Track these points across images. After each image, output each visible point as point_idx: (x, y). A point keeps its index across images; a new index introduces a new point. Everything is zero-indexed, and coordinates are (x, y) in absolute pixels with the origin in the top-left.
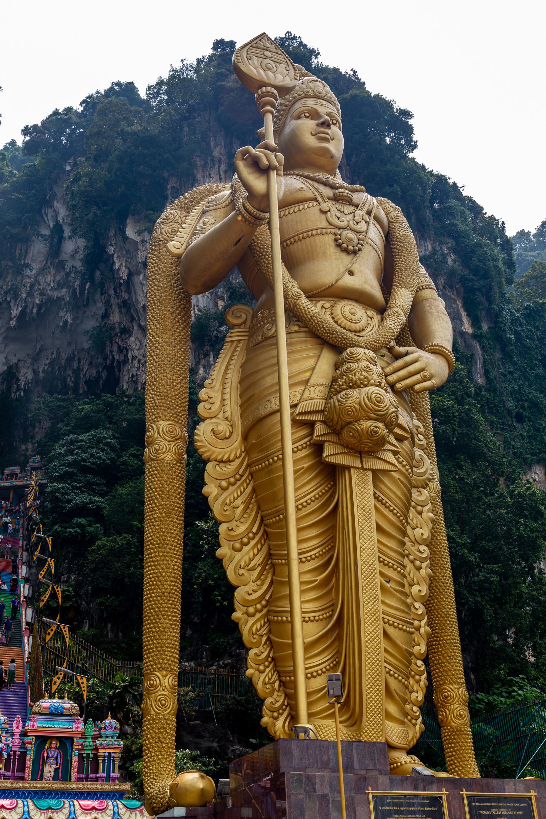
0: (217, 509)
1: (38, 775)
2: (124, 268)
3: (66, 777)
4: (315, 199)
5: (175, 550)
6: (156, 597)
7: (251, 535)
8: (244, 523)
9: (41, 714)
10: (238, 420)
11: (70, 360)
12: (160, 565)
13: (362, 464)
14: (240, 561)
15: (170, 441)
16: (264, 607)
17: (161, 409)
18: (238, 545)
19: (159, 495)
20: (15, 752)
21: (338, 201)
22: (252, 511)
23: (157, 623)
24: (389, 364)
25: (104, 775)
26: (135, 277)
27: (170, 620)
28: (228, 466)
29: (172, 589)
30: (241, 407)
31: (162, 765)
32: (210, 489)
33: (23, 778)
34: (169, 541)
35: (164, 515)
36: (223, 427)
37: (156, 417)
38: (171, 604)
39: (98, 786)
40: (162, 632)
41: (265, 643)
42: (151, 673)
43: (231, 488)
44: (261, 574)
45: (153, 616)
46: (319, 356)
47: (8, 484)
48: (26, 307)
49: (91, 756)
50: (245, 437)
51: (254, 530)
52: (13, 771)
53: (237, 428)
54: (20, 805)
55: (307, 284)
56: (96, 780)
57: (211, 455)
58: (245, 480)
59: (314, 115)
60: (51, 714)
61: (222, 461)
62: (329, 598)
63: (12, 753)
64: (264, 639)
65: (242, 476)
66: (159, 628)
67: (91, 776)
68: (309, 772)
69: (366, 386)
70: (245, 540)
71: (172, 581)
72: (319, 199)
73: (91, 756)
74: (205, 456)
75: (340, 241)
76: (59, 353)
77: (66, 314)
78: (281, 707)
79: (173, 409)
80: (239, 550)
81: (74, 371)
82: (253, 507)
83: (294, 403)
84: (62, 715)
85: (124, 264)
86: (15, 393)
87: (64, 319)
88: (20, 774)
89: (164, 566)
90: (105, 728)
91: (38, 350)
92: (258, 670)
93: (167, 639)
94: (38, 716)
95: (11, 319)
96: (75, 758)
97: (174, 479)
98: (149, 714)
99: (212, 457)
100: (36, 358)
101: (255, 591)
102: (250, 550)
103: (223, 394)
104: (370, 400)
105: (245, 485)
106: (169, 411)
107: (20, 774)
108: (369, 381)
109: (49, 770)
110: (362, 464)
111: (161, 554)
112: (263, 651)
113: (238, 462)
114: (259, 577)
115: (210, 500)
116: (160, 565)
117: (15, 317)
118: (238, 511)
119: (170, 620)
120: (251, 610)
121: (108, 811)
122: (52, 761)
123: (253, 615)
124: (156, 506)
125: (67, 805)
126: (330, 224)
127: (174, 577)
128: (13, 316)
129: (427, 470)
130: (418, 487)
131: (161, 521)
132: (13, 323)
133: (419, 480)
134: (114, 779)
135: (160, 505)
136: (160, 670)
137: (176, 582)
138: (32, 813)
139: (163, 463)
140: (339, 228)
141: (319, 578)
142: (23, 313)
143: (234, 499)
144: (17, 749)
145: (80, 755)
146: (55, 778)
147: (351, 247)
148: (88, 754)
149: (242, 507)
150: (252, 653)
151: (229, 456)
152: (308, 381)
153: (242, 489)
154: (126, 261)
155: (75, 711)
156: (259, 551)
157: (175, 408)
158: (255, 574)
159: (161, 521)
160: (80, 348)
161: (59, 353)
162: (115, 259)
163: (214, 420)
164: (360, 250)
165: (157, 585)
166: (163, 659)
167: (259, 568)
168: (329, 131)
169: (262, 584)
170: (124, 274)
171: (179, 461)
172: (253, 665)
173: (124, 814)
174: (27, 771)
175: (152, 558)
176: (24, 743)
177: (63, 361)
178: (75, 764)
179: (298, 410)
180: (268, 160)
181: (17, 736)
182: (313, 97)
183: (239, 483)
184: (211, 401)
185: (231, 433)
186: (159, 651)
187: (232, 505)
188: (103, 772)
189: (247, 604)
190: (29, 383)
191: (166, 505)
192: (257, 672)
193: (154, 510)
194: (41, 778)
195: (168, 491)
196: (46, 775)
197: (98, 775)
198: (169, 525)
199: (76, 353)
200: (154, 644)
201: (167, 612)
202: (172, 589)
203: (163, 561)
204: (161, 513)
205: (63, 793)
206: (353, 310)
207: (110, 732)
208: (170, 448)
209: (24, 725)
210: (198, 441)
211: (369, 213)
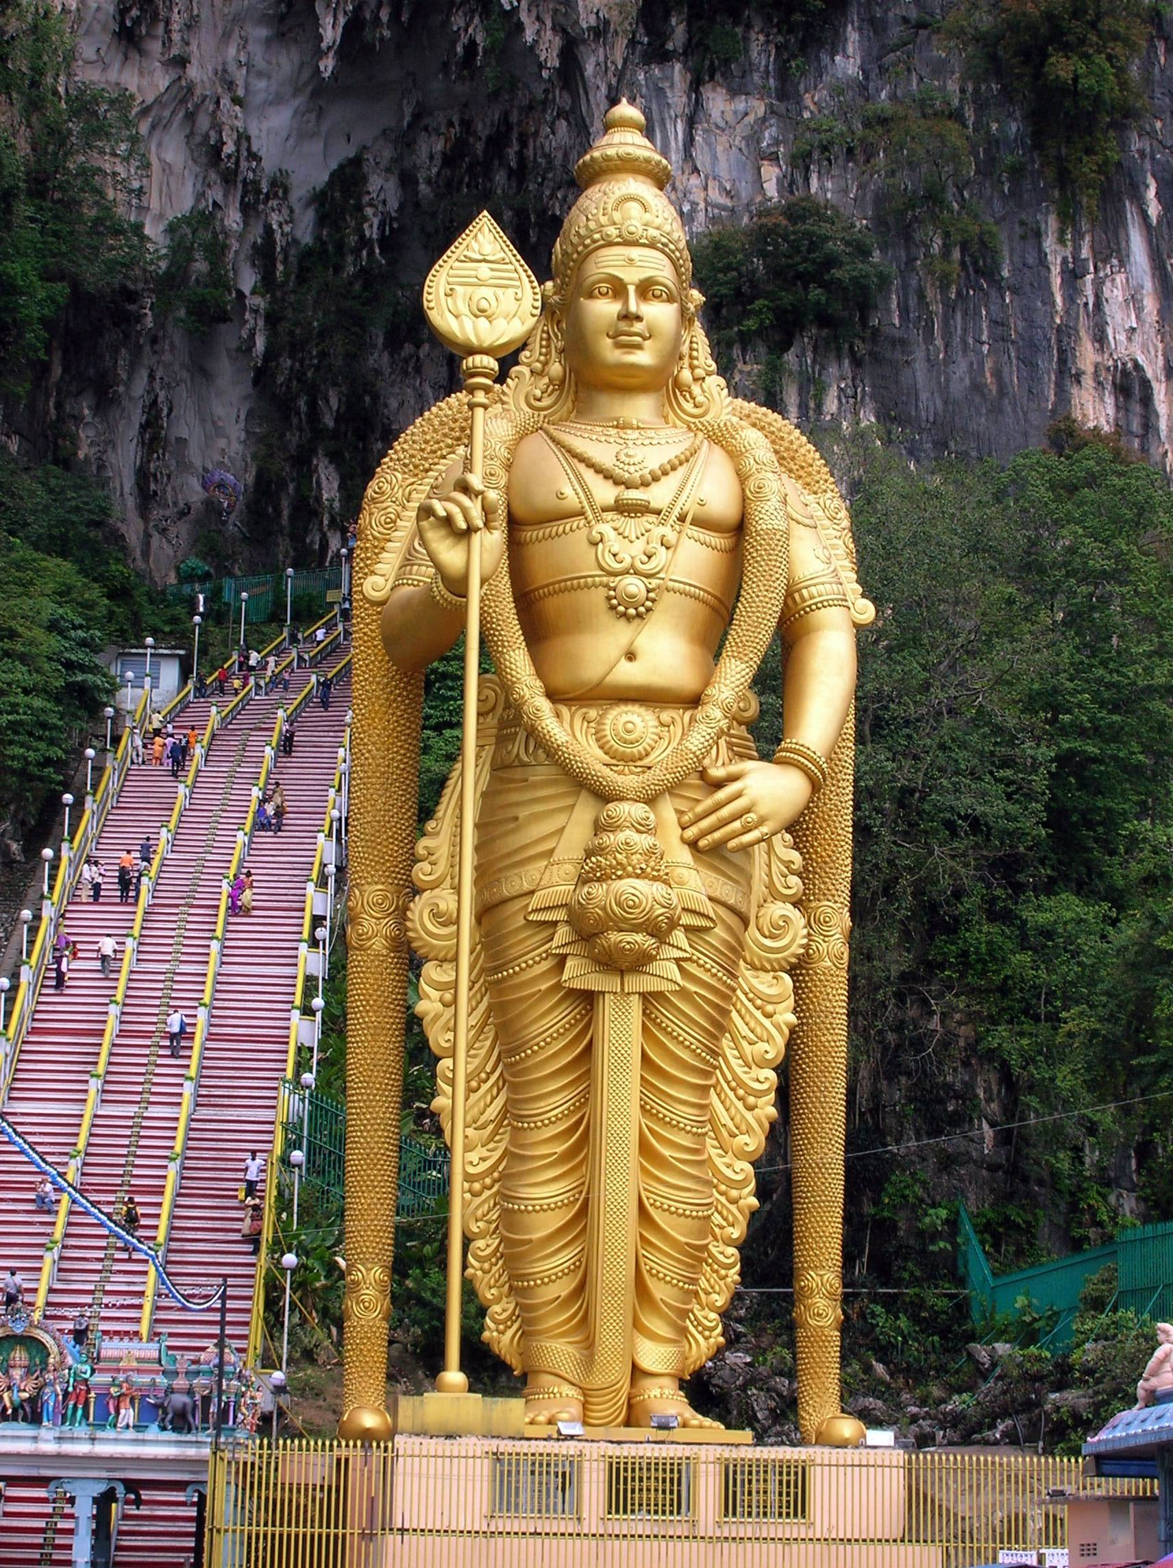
2: (549, 34)
4: (582, 513)
7: (483, 1075)
11: (497, 143)
13: (622, 984)
16: (495, 1181)
21: (621, 513)
24: (698, 801)
26: (582, 48)
44: (495, 1133)
46: (573, 806)
48: (358, 9)
55: (560, 680)
59: (618, 289)
62: (578, 1174)
69: (620, 877)
72: (589, 513)
75: (614, 602)
76: (467, 124)
77: (472, 19)
78: (509, 1318)
81: (511, 173)
82: (490, 1032)
85: (549, 24)
86: (357, 252)
87: (464, 40)
91: (407, 119)
95: (320, 54)
100: (405, 140)
101: (483, 1159)
104: (619, 904)
108: (624, 869)
110: (622, 984)
114: (491, 1139)
117: (329, 48)
120: (477, 1186)
126: (602, 569)
128: (324, 45)
129: (793, 941)
130: (774, 970)
132: (327, 65)
133: (777, 960)
140: (615, 574)
141: (560, 1149)
142: (354, 28)
147: (632, 611)
152: (551, 852)
154: (556, 11)
160: (525, 102)
161: (467, 124)
162: (524, 17)
163: (437, 891)
164: (649, 610)
167: (491, 1127)
168: (638, 327)
170: (550, 53)
177: (479, 147)
179: (535, 902)
180: (466, 520)
182: (618, 244)
184: (432, 858)
190: (392, 219)
192: (479, 1273)
199: (514, 118)
206: (630, 726)
211: (682, 519)
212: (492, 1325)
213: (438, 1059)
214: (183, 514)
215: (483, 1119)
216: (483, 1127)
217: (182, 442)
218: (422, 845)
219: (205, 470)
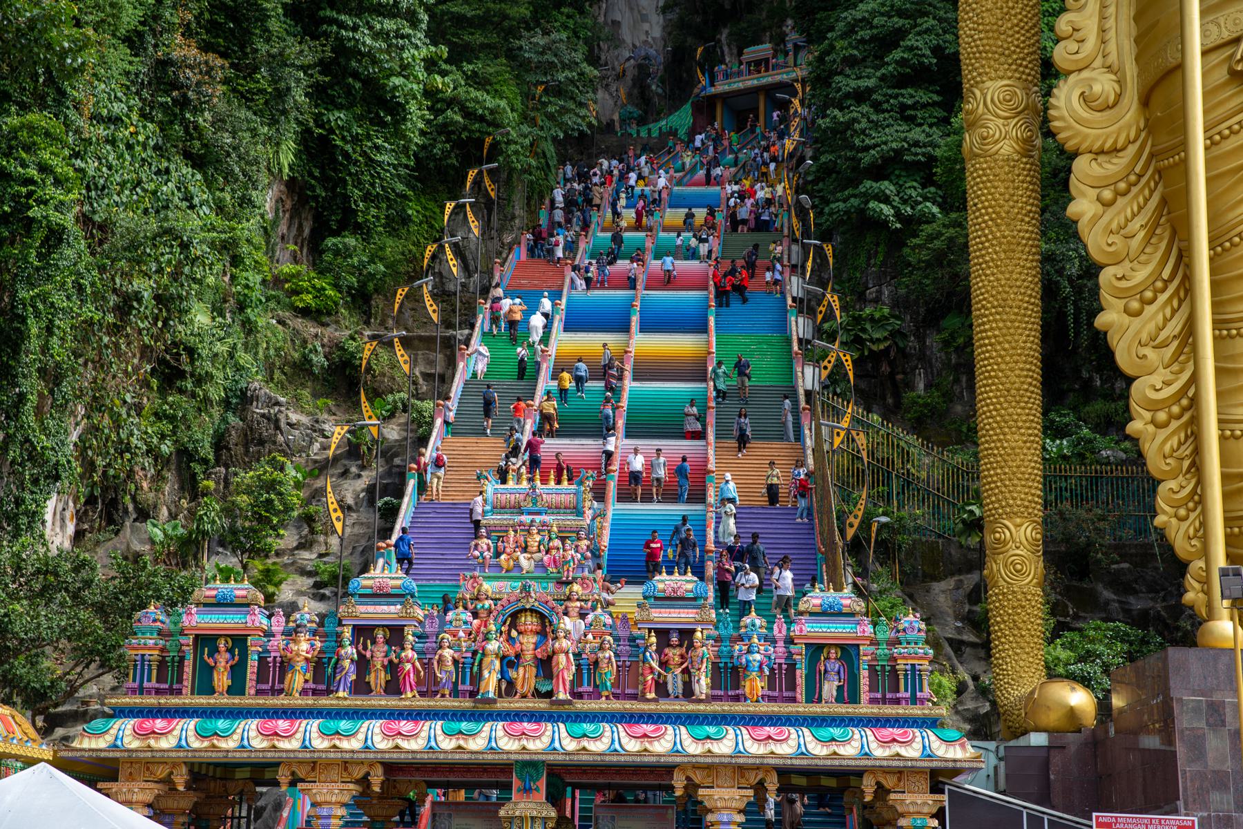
0: (1096, 242)
1: (814, 696)
3: (854, 699)
5: (1025, 315)
6: (996, 397)
7: (1159, 284)
8: (1146, 263)
9: (811, 614)
10: (1131, 70)
12: (1000, 343)
14: (1138, 332)
15: (1006, 118)
17: (986, 58)
18: (1135, 305)
19: (992, 219)
20: (780, 664)
22: (1161, 240)
23: (1000, 440)
25: (908, 695)
27: (1023, 435)
28: (1115, 161)
29: (1023, 383)
30: (1137, 41)
31: (1022, 663)
32: (1082, 207)
33: (793, 700)
34: (1014, 300)
35: (1003, 256)
36: (1104, 85)
37: (980, 74)
38: (1023, 408)
39: (900, 710)
40: (1009, 455)
41: (1188, 471)
42: (996, 521)
43: (1121, 201)
45: (993, 429)
47: (752, 82)
49: (888, 668)
50: (1145, 102)
51: (1166, 275)
52: (781, 690)
53: (1129, 84)
54: (794, 736)
56: (897, 701)
57: (1081, 143)
58: (1148, 183)
60: (824, 613)
61: (1101, 152)
63: (776, 666)
64: (1186, 463)
65: (1140, 176)
66: (1004, 448)
67: (889, 696)
68: (1217, 697)
70: (1149, 294)
71: (1022, 369)
73: (888, 668)
74: (1070, 146)
79: (1009, 56)
80: (1137, 314)
83: (1235, 35)
84: (840, 614)
88: (790, 694)
89: (1007, 346)
90: (904, 630)
92: (1176, 516)
93: (1018, 467)
94: (807, 617)
96: (864, 673)
97: (1018, 188)
98: (996, 585)
99: (1083, 147)
101: (1167, 384)
102: (1157, 312)
103: (1103, 18)
105: (1147, 192)
106: (1002, 59)
107: (790, 694)
109: (829, 688)
111: (1001, 325)
112: (1184, 484)
113: (1132, 150)
115: (1082, 227)
116: (1000, 343)
118: (1135, 243)
119: (1023, 435)
120: (1162, 416)
121: (914, 745)
122: (833, 676)
123: (1165, 425)
124: (988, 241)
125: (857, 736)
127: (1025, 362)
131: (997, 266)
134: (922, 701)
135: (995, 238)
136: (1009, 516)
137: (1029, 370)
138: (810, 747)
139: (995, 161)
143: (1127, 221)
144: (783, 661)
145: (872, 668)
146: (839, 699)
148: (883, 666)
149: (1142, 233)
150: (1162, 489)
151: (1116, 142)
153: (1141, 199)
155: (858, 609)
156: (1174, 312)
157: (1014, 52)
158: (1169, 352)
159: (997, 266)
163: (1085, 74)
165: (996, 377)
166: (1014, 499)
167: (1176, 343)
169: (1181, 371)
171: (1026, 153)
172: (1167, 508)
173: (938, 749)
174: (798, 690)
175: (985, 331)
176: (790, 654)
178: (864, 681)
181: (781, 644)
183: (1135, 190)
184: (1078, 35)
185: (1119, 96)
186: (1006, 486)
187: (1122, 232)
188: (906, 690)
189: (1154, 406)
191: (1005, 237)
192: (1174, 521)
193: (985, 248)
194: (819, 700)
195: (1008, 212)
196: (825, 695)
197: (898, 695)
198: (1012, 272)
200: (997, 474)
201: (1016, 421)
202: (1023, 383)
203: (1004, 335)
204: (996, 253)
205: (851, 720)
207: (911, 636)
208: (1007, 132)
209: (789, 629)
210: (1057, 119)
212: (1196, 585)
213: (1101, 267)
214: (620, 77)
215: (1163, 335)
216: (1164, 345)
217: (616, 24)
218: (1063, 24)
219: (634, 45)
